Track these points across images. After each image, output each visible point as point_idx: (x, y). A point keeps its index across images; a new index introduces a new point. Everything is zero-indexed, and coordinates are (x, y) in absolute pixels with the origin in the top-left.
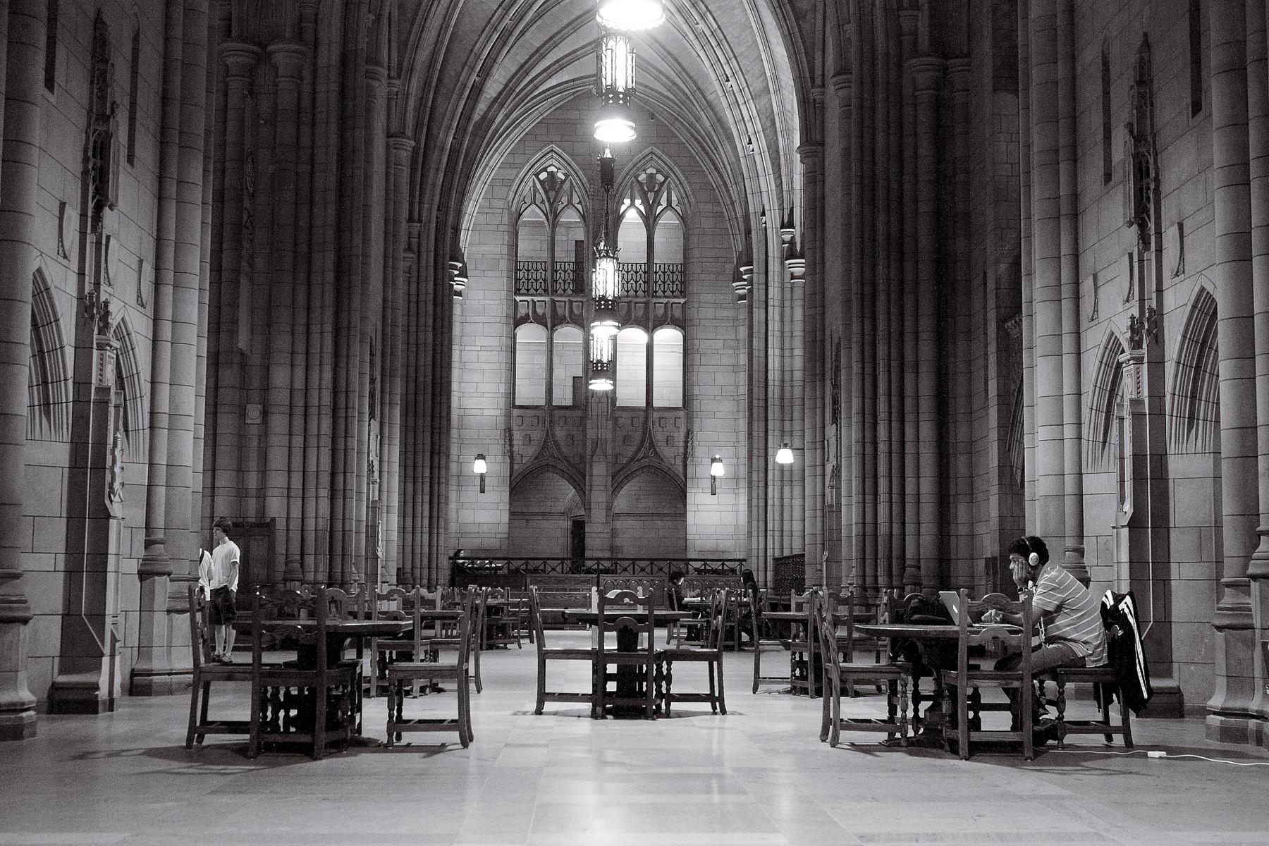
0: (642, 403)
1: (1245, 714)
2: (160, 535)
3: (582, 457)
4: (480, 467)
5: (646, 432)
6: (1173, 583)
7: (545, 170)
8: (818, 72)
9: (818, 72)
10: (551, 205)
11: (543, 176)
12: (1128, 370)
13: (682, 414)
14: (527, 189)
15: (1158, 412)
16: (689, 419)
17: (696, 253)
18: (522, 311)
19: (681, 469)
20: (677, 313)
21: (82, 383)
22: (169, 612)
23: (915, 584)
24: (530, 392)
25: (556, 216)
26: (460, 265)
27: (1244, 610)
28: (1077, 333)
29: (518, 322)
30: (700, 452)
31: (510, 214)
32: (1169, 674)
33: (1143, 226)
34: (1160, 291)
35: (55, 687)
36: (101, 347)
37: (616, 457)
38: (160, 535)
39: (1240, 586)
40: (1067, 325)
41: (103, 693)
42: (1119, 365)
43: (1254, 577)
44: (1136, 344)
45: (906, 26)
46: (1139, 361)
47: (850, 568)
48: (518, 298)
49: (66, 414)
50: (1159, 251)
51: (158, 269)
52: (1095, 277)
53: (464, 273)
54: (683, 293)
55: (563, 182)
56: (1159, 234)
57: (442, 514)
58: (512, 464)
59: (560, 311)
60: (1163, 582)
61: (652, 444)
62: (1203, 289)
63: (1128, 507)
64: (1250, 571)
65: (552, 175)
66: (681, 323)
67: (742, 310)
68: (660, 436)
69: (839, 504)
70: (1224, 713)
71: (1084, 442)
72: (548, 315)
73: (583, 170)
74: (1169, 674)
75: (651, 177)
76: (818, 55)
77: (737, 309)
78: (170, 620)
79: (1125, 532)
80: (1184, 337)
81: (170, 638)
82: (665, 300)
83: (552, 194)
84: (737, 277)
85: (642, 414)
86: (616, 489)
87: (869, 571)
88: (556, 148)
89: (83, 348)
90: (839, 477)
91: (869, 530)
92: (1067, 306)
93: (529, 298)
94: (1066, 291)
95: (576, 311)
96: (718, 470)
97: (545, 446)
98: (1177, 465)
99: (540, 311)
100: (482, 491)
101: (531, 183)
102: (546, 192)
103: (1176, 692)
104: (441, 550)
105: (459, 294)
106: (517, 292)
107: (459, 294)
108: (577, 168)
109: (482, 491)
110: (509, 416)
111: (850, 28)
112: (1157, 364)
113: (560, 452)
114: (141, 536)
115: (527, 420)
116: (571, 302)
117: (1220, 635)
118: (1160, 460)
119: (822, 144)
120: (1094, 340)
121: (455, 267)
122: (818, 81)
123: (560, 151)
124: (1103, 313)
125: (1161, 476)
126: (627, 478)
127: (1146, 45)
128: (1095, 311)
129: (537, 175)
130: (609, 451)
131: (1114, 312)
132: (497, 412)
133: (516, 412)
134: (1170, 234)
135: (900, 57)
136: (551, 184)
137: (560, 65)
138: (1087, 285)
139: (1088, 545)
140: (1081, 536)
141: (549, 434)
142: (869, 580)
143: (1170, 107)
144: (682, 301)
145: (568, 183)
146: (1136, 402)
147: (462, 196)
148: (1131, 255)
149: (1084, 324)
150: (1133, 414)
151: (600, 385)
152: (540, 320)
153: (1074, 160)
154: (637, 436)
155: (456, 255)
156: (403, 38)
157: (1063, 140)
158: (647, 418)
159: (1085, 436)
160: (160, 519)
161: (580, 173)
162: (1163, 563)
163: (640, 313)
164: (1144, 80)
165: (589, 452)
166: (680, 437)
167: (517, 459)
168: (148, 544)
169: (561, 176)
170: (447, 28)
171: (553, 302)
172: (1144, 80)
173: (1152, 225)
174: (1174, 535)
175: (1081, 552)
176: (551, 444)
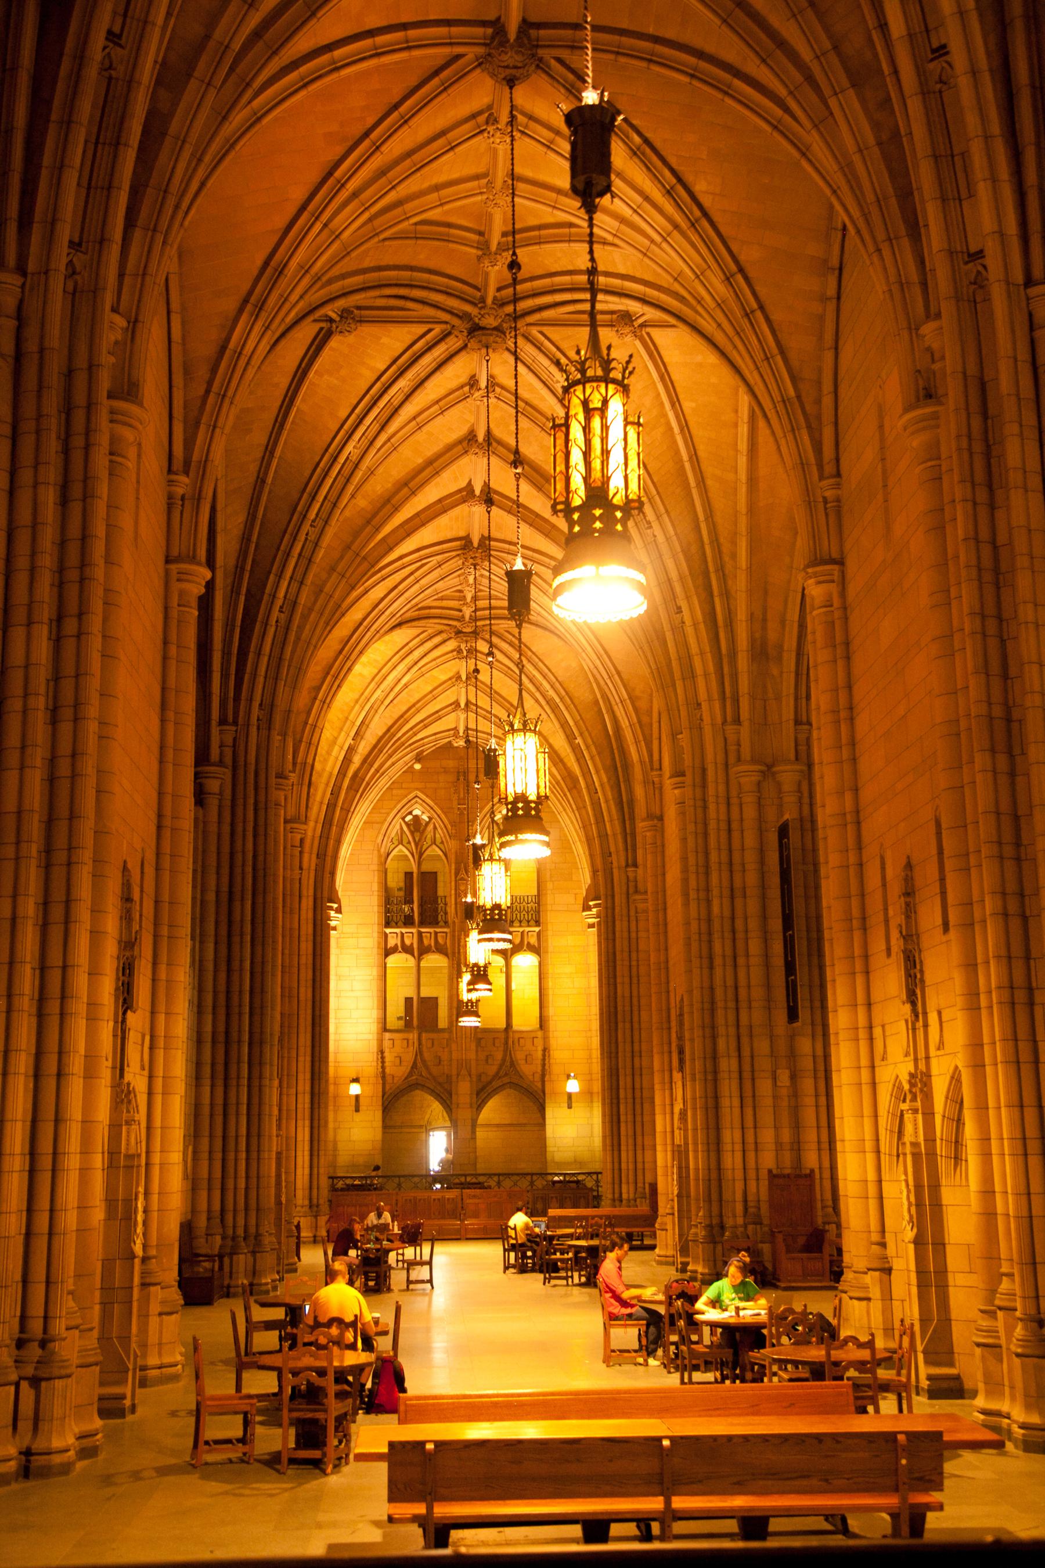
0: (503, 1025)
1: (998, 1414)
2: (153, 1252)
3: (449, 1077)
4: (355, 1089)
6: (951, 1290)
7: (410, 813)
8: (656, 757)
9: (656, 757)
10: (417, 845)
11: (409, 818)
12: (908, 1117)
14: (394, 831)
15: (932, 1154)
16: (546, 1038)
17: (550, 885)
18: (392, 942)
19: (539, 1085)
20: (533, 941)
22: (160, 1314)
23: (755, 1223)
25: (421, 855)
26: (335, 906)
27: (992, 1332)
28: (873, 1067)
29: (388, 952)
30: (556, 1069)
31: (380, 856)
32: (951, 1364)
33: (914, 1004)
34: (927, 1058)
36: (128, 1123)
37: (479, 1076)
39: (991, 1314)
40: (864, 1061)
41: (127, 1402)
42: (902, 1115)
43: (1000, 1308)
44: (914, 1099)
45: (732, 738)
46: (915, 1111)
47: (699, 1209)
48: (388, 931)
50: (926, 1026)
52: (883, 1026)
53: (339, 910)
54: (538, 923)
55: (427, 824)
56: (925, 1013)
57: (322, 1136)
58: (384, 1084)
59: (426, 942)
60: (943, 1288)
61: (513, 1064)
62: (956, 1067)
63: (915, 1230)
64: (997, 1302)
65: (416, 817)
66: (536, 950)
68: (519, 1056)
69: (686, 1144)
70: (984, 1412)
71: (882, 1156)
72: (415, 946)
73: (445, 813)
74: (951, 1364)
76: (655, 743)
78: (161, 1322)
79: (912, 1246)
80: (947, 1098)
81: (160, 1337)
84: (586, 908)
85: (503, 1036)
86: (480, 1107)
88: (420, 794)
90: (686, 1121)
92: (863, 1045)
93: (397, 930)
94: (862, 1034)
95: (441, 940)
96: (573, 1086)
97: (414, 1066)
98: (948, 1195)
99: (408, 942)
100: (357, 1110)
101: (398, 827)
102: (412, 833)
103: (957, 1378)
104: (322, 1171)
105: (334, 928)
106: (388, 924)
107: (334, 928)
108: (439, 812)
109: (357, 1110)
110: (380, 1041)
111: (684, 739)
112: (929, 1115)
115: (397, 1043)
116: (436, 933)
117: (978, 1351)
118: (935, 1187)
119: (661, 819)
120: (886, 1075)
121: (331, 908)
122: (656, 765)
123: (423, 797)
124: (891, 1059)
125: (937, 1205)
126: (489, 1097)
127: (909, 866)
128: (885, 1052)
129: (403, 819)
130: (474, 1072)
131: (897, 1068)
132: (370, 1037)
133: (387, 1035)
134: (933, 1018)
135: (726, 765)
136: (416, 825)
137: (425, 724)
138: (877, 1032)
139: (889, 1238)
140: (883, 1232)
141: (420, 1052)
143: (929, 916)
144: (537, 929)
145: (431, 826)
146: (915, 1145)
147: (339, 842)
148: (907, 1021)
149: (877, 1063)
150: (913, 1154)
151: (468, 1022)
152: (407, 950)
153: (864, 929)
154: (499, 1055)
155: (333, 897)
156: (298, 737)
158: (507, 1038)
159: (882, 1149)
161: (443, 816)
162: (942, 1272)
164: (909, 892)
165: (454, 1072)
167: (389, 1079)
169: (425, 817)
171: (420, 934)
172: (909, 892)
173: (919, 1004)
174: (949, 1249)
175: (883, 1245)
176: (419, 1064)
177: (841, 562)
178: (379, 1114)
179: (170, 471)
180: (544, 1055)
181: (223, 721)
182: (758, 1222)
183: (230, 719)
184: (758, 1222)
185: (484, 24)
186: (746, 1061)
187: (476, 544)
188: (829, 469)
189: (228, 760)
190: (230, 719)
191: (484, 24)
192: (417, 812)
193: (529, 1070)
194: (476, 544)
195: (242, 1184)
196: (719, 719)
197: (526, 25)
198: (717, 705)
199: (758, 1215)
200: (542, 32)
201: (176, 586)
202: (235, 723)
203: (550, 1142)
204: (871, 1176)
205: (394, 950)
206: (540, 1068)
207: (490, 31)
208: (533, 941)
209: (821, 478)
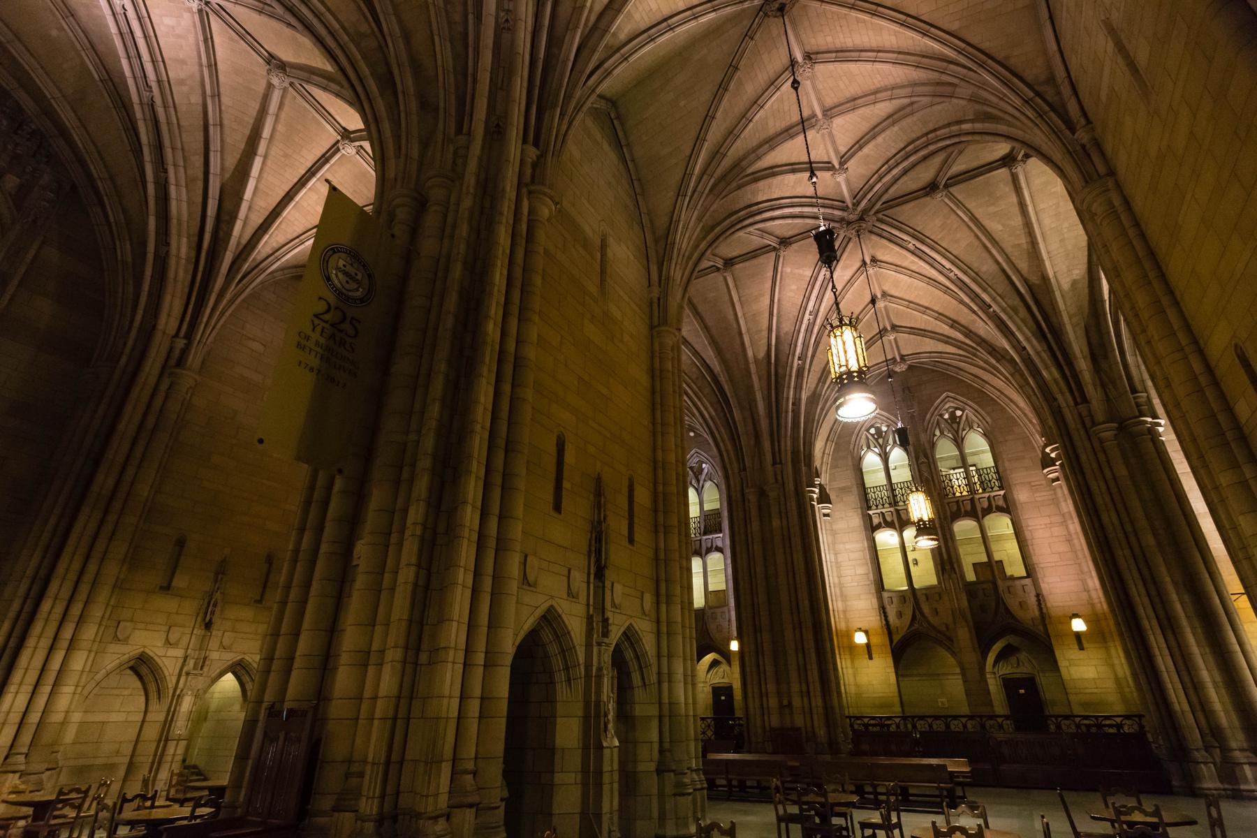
16: (1036, 584)
19: (1041, 628)
20: (1001, 503)
24: (895, 578)
54: (1001, 488)
61: (1008, 611)
67: (1059, 492)
68: (1012, 603)
82: (986, 495)
83: (881, 441)
99: (889, 519)
106: (869, 508)
110: (880, 598)
113: (929, 623)
144: (1002, 493)
152: (890, 525)
163: (969, 507)
166: (1032, 600)
169: (884, 429)
170: (510, 72)
171: (897, 511)
178: (890, 661)
180: (1039, 601)
205: (879, 527)
206: (1037, 613)
208: (1001, 503)
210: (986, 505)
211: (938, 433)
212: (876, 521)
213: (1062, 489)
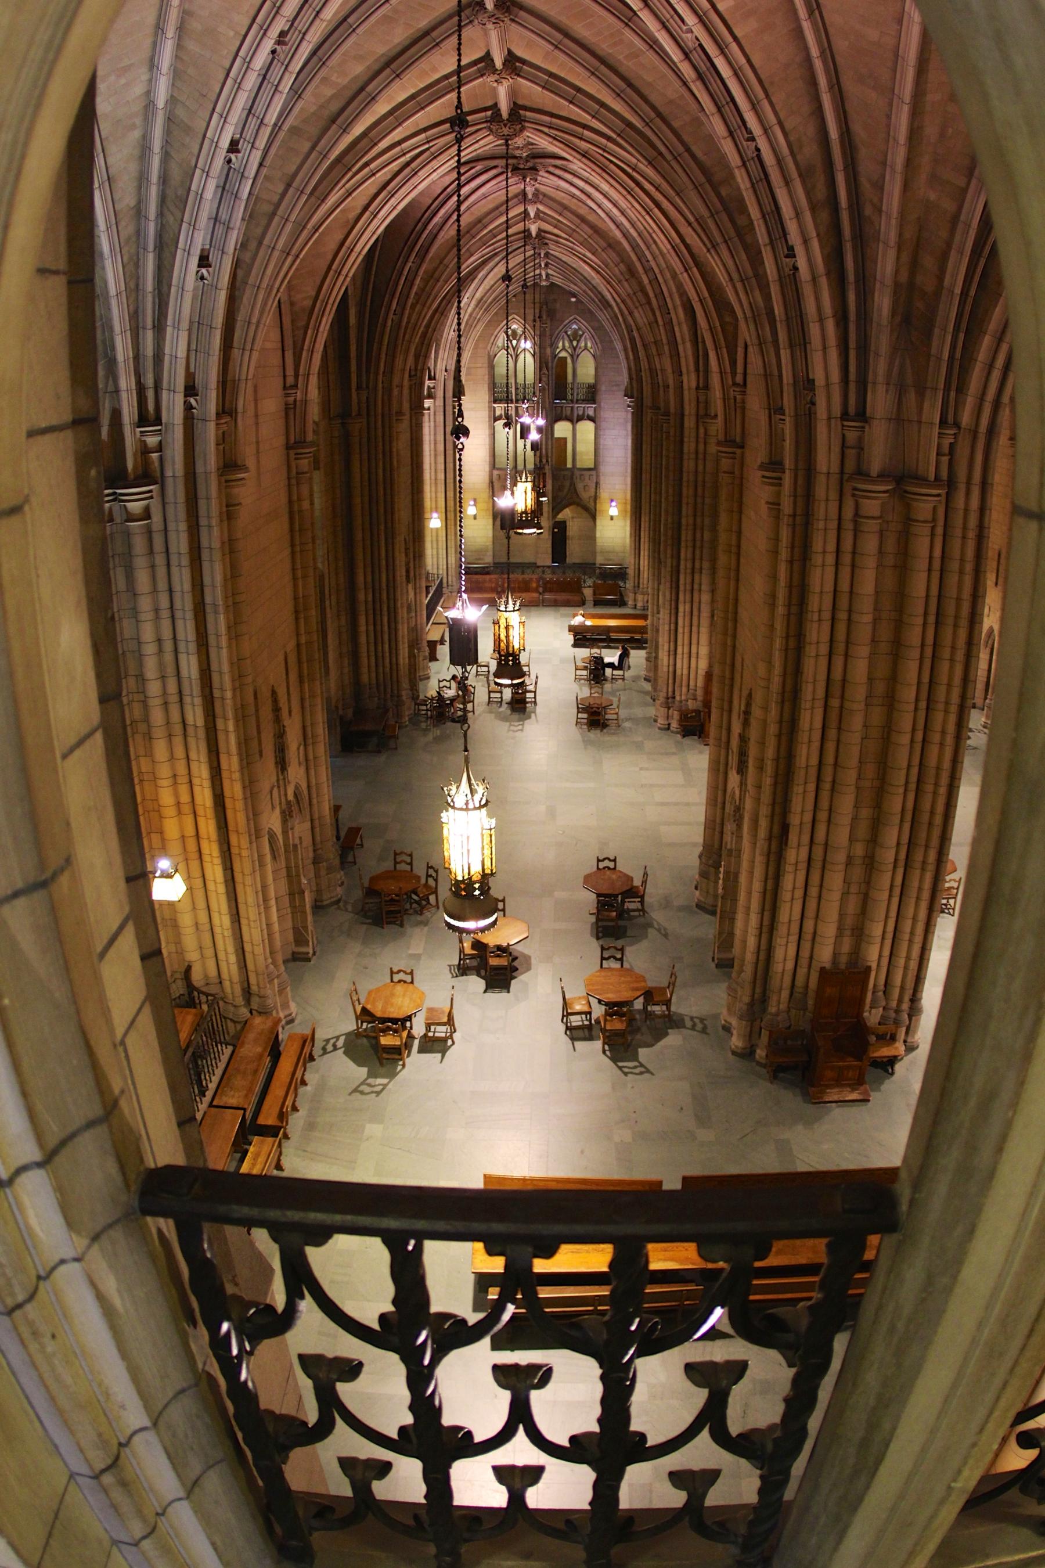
5: (573, 485)
13: (594, 473)
16: (598, 476)
18: (498, 413)
20: (591, 413)
21: (286, 845)
29: (496, 419)
30: (604, 495)
35: (293, 953)
38: (319, 846)
49: (283, 858)
51: (305, 745)
54: (593, 401)
68: (580, 486)
75: (575, 332)
77: (627, 411)
87: (670, 690)
89: (285, 832)
91: (671, 669)
106: (495, 402)
114: (311, 849)
142: (670, 694)
157: (728, 674)
160: (318, 838)
163: (569, 413)
168: (314, 851)
177: (742, 447)
179: (285, 388)
181: (359, 388)
182: (695, 699)
183: (364, 386)
184: (695, 699)
185: (485, 109)
186: (696, 605)
187: (534, 234)
188: (739, 379)
189: (364, 412)
190: (364, 386)
191: (485, 109)
192: (514, 326)
193: (585, 495)
194: (534, 234)
195: (388, 670)
196: (694, 385)
197: (516, 108)
198: (693, 376)
199: (695, 695)
200: (528, 114)
201: (293, 464)
202: (368, 387)
203: (599, 542)
204: (718, 821)
207: (489, 113)
209: (735, 384)
210: (581, 413)
211: (560, 345)
212: (498, 413)
213: (630, 416)
